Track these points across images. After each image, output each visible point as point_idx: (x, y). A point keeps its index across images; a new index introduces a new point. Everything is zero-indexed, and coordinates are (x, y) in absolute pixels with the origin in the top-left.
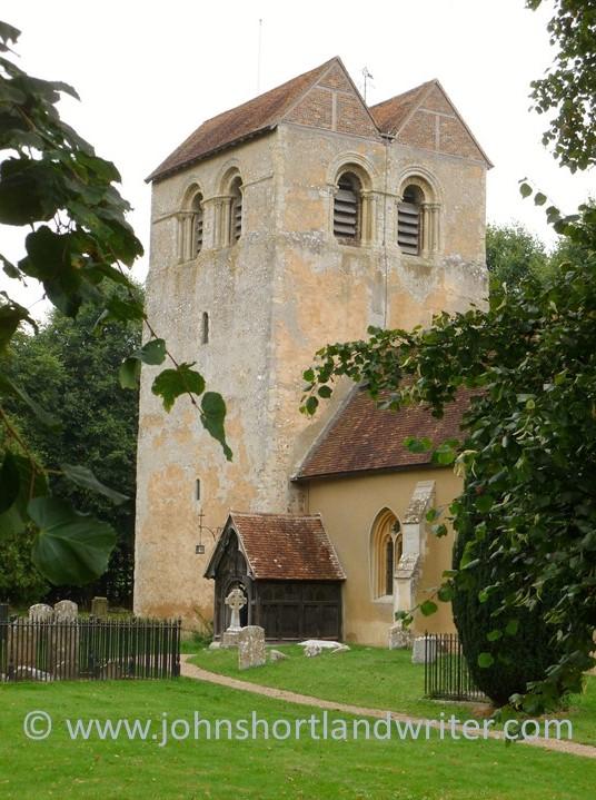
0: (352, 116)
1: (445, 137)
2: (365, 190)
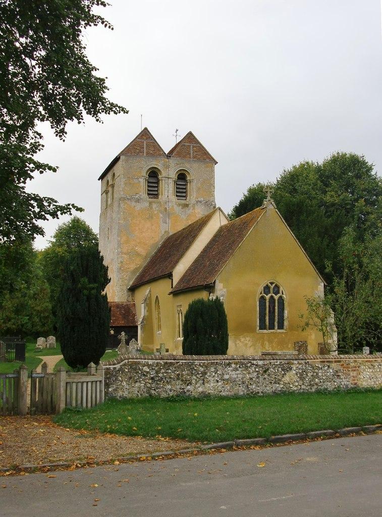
1: (196, 153)
2: (160, 177)
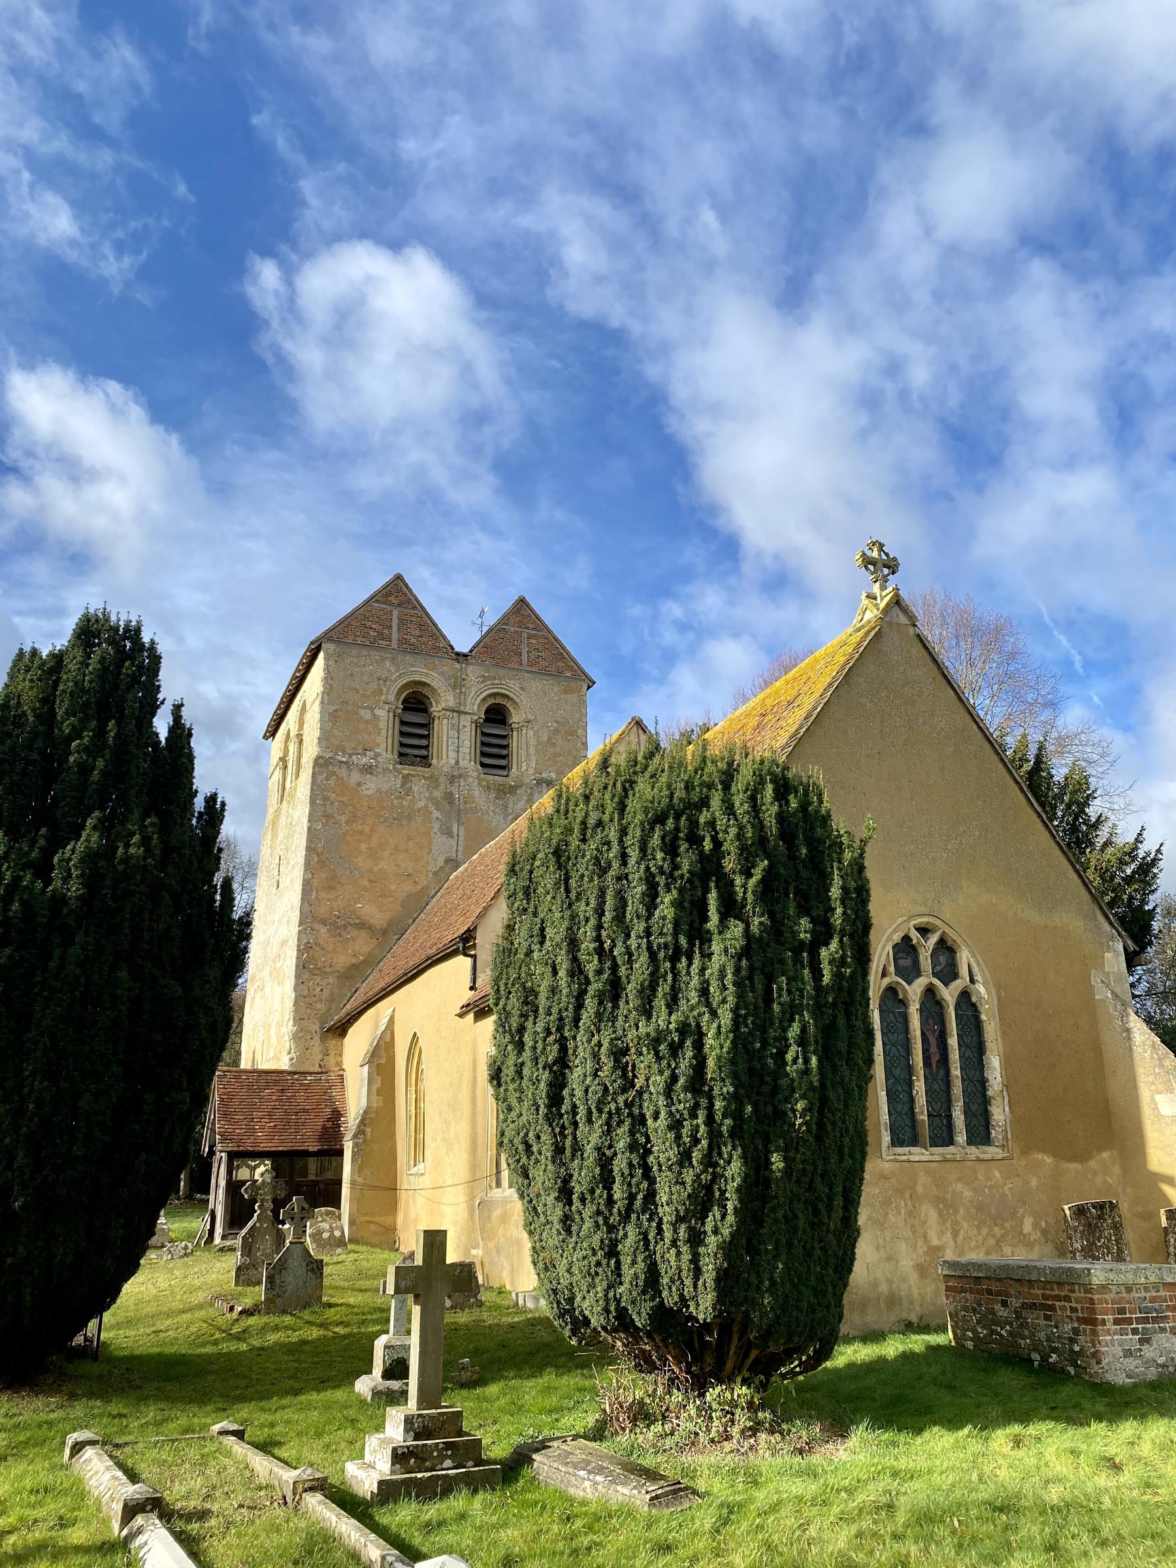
0: (418, 634)
1: (534, 654)
